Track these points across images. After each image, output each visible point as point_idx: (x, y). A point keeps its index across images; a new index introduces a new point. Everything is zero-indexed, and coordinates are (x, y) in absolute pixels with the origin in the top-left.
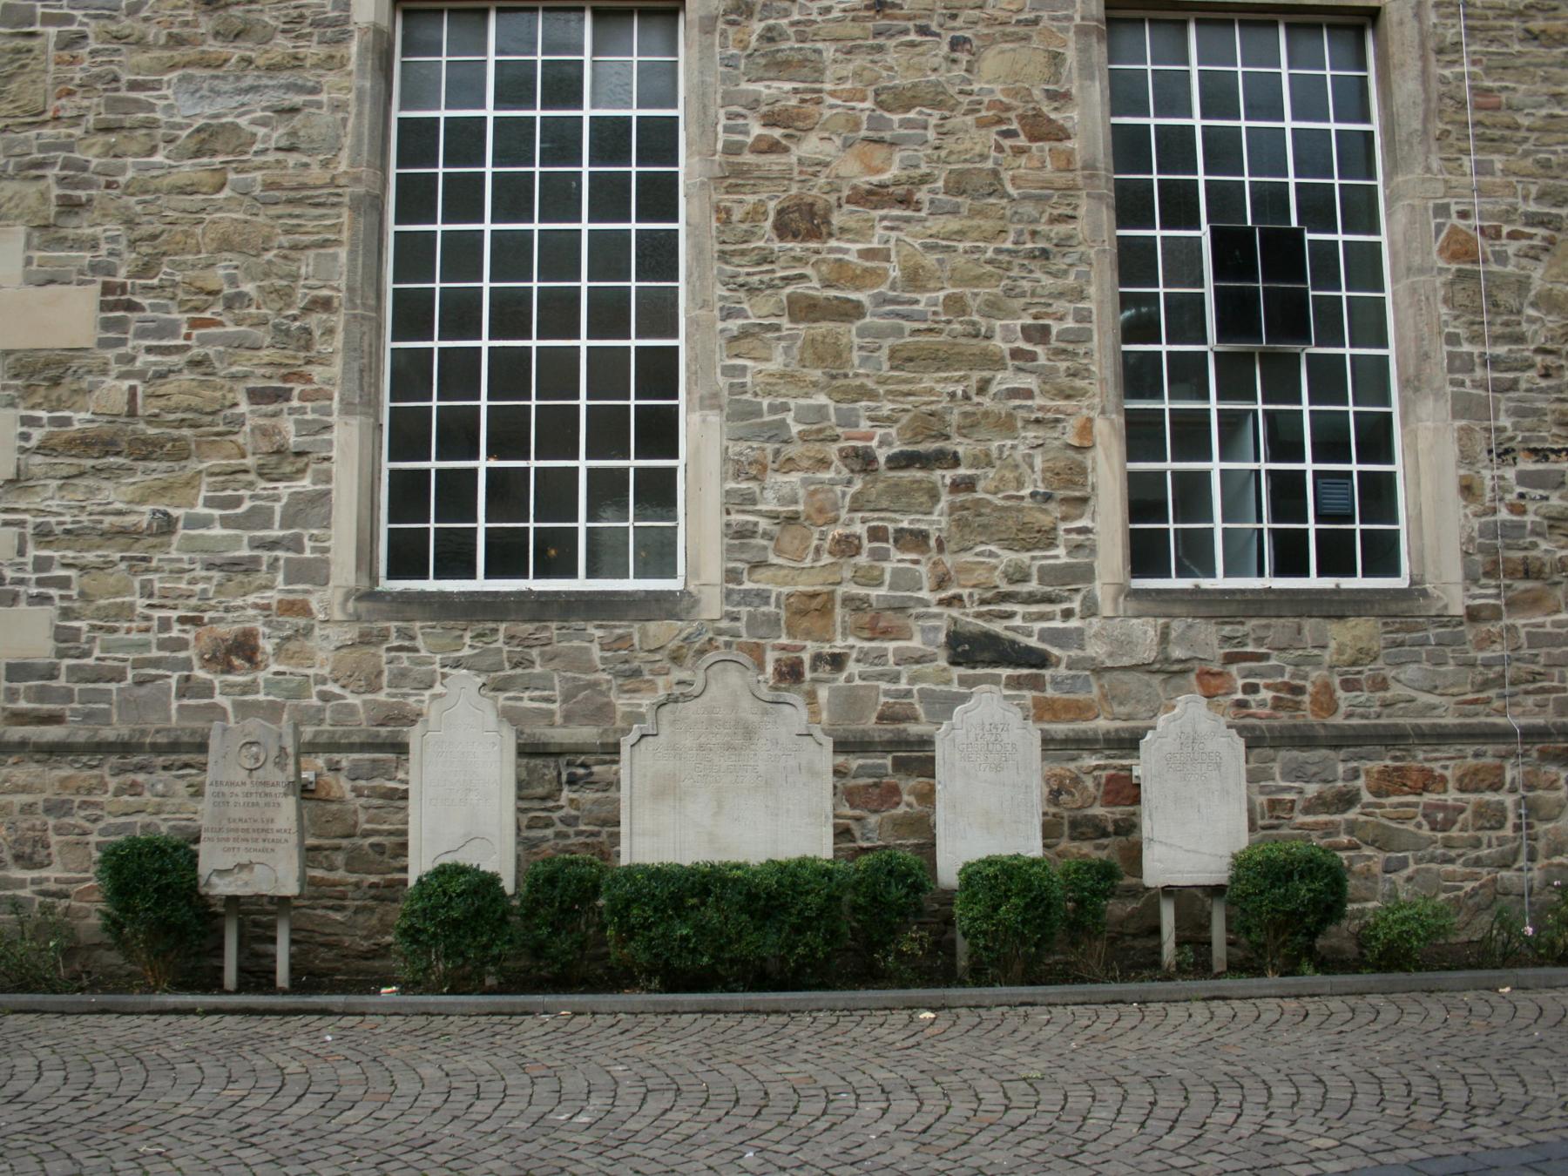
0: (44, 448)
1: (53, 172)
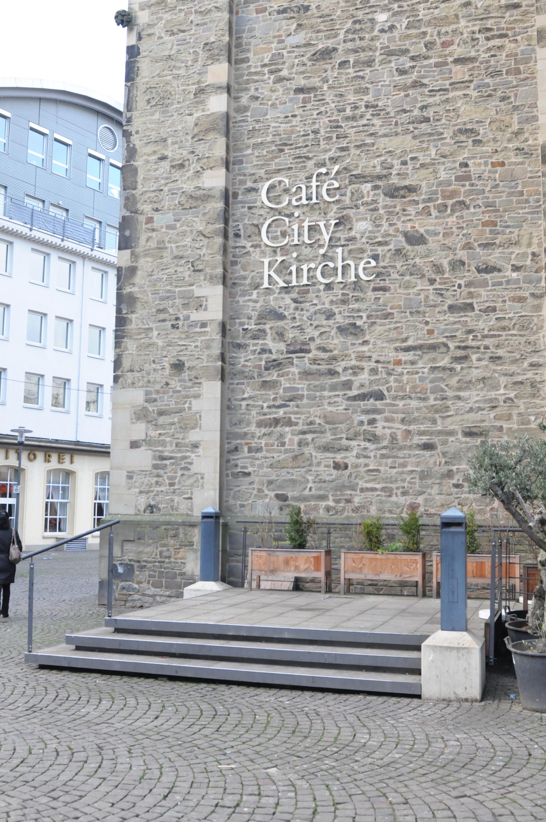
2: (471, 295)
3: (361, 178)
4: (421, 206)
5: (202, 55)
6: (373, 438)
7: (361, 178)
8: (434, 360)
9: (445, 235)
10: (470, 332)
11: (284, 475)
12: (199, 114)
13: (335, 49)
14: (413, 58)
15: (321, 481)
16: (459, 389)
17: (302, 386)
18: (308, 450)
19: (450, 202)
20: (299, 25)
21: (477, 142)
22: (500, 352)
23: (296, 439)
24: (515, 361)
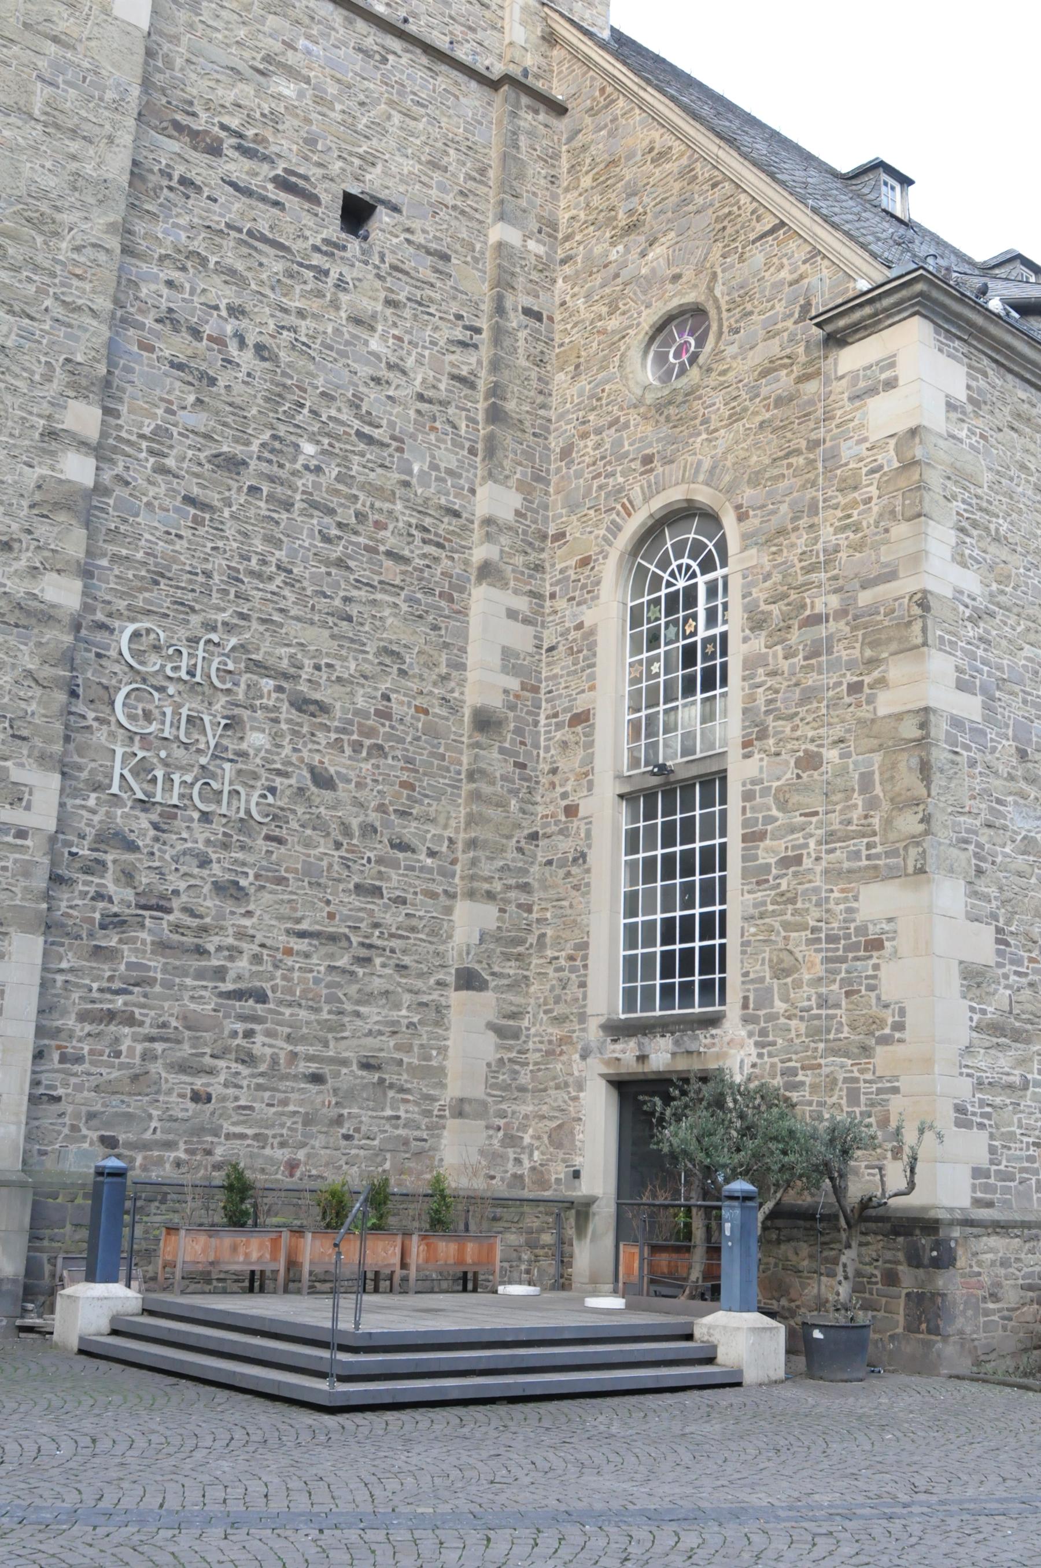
0: (977, 1029)
1: (972, 847)
2: (380, 875)
3: (259, 667)
4: (333, 736)
5: (60, 376)
6: (248, 1059)
7: (259, 667)
8: (332, 956)
9: (359, 785)
10: (376, 925)
11: (115, 1104)
12: (46, 471)
13: (244, 463)
14: (340, 525)
15: (173, 1119)
16: (358, 1002)
17: (156, 964)
18: (156, 1068)
19: (367, 742)
20: (198, 400)
21: (402, 673)
22: (407, 960)
23: (139, 1048)
24: (421, 975)
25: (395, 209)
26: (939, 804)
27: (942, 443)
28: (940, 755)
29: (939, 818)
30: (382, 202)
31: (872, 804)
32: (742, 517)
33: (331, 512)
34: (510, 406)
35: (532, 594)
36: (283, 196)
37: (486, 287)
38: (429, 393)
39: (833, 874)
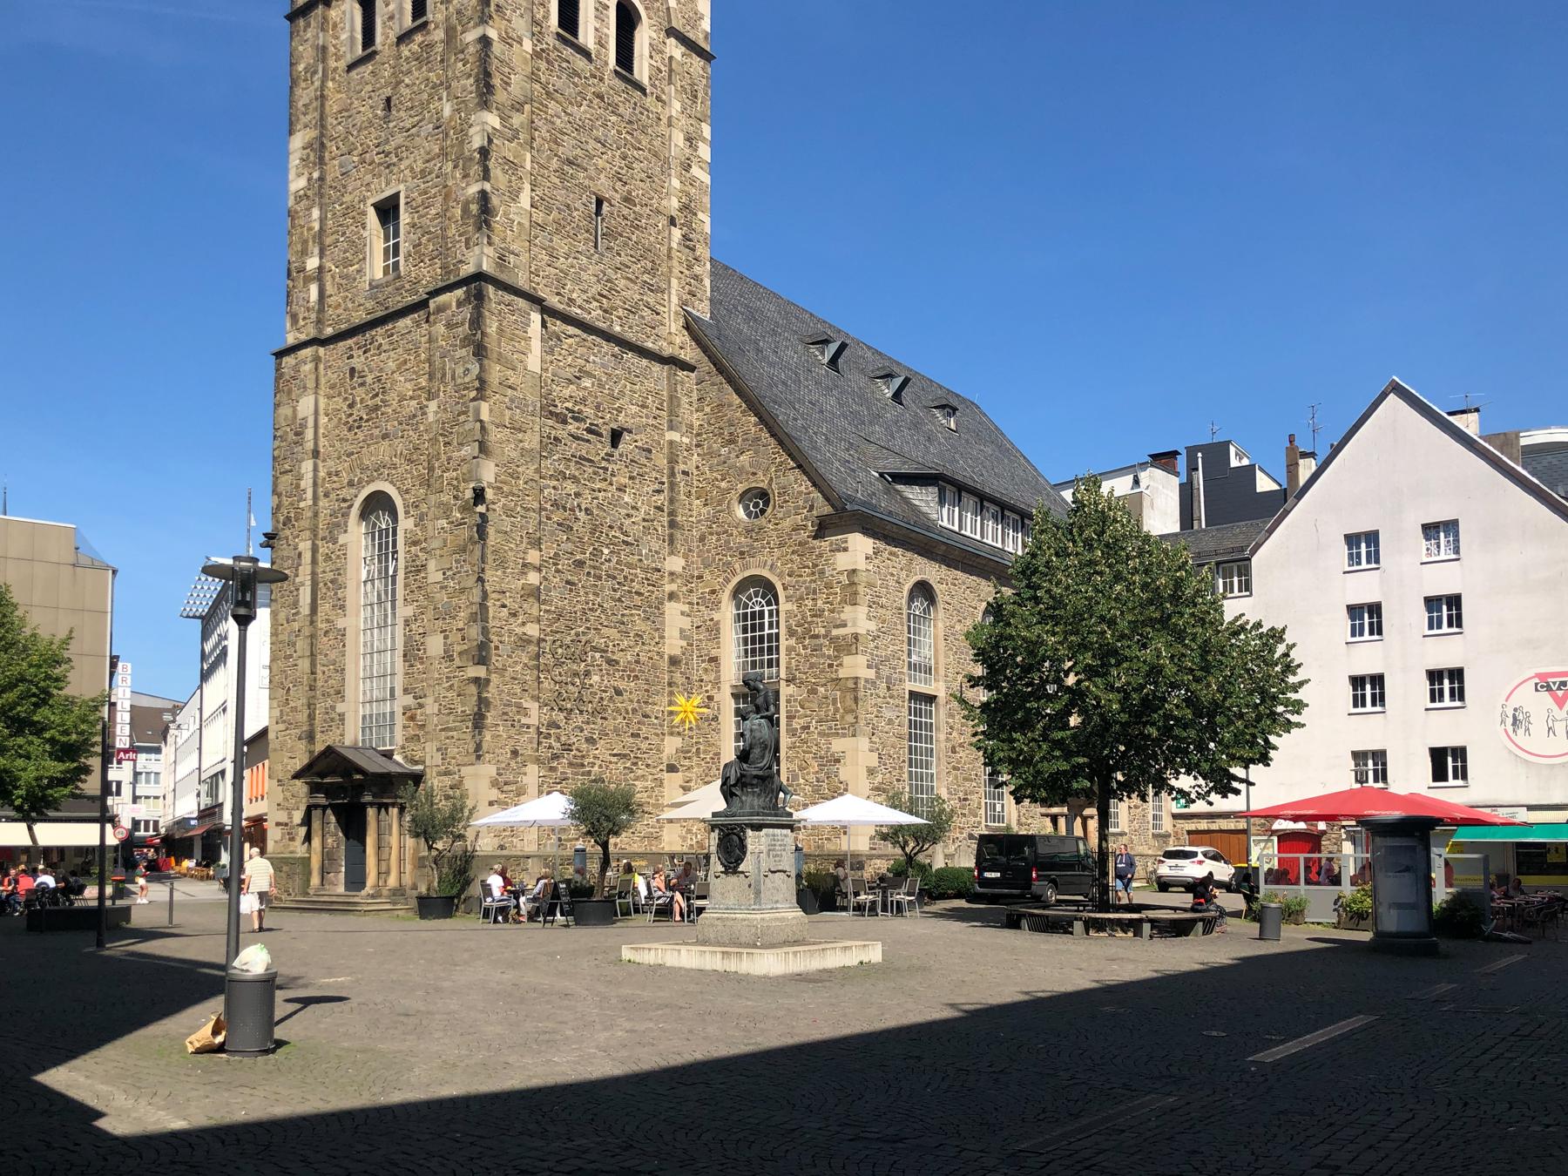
3: (595, 649)
7: (595, 649)
8: (624, 763)
14: (618, 583)
17: (569, 771)
25: (630, 432)
26: (861, 713)
27: (864, 574)
28: (861, 694)
29: (860, 716)
30: (625, 429)
31: (837, 710)
32: (785, 589)
33: (615, 578)
34: (679, 519)
35: (689, 603)
36: (590, 437)
37: (665, 461)
38: (647, 517)
39: (822, 734)
